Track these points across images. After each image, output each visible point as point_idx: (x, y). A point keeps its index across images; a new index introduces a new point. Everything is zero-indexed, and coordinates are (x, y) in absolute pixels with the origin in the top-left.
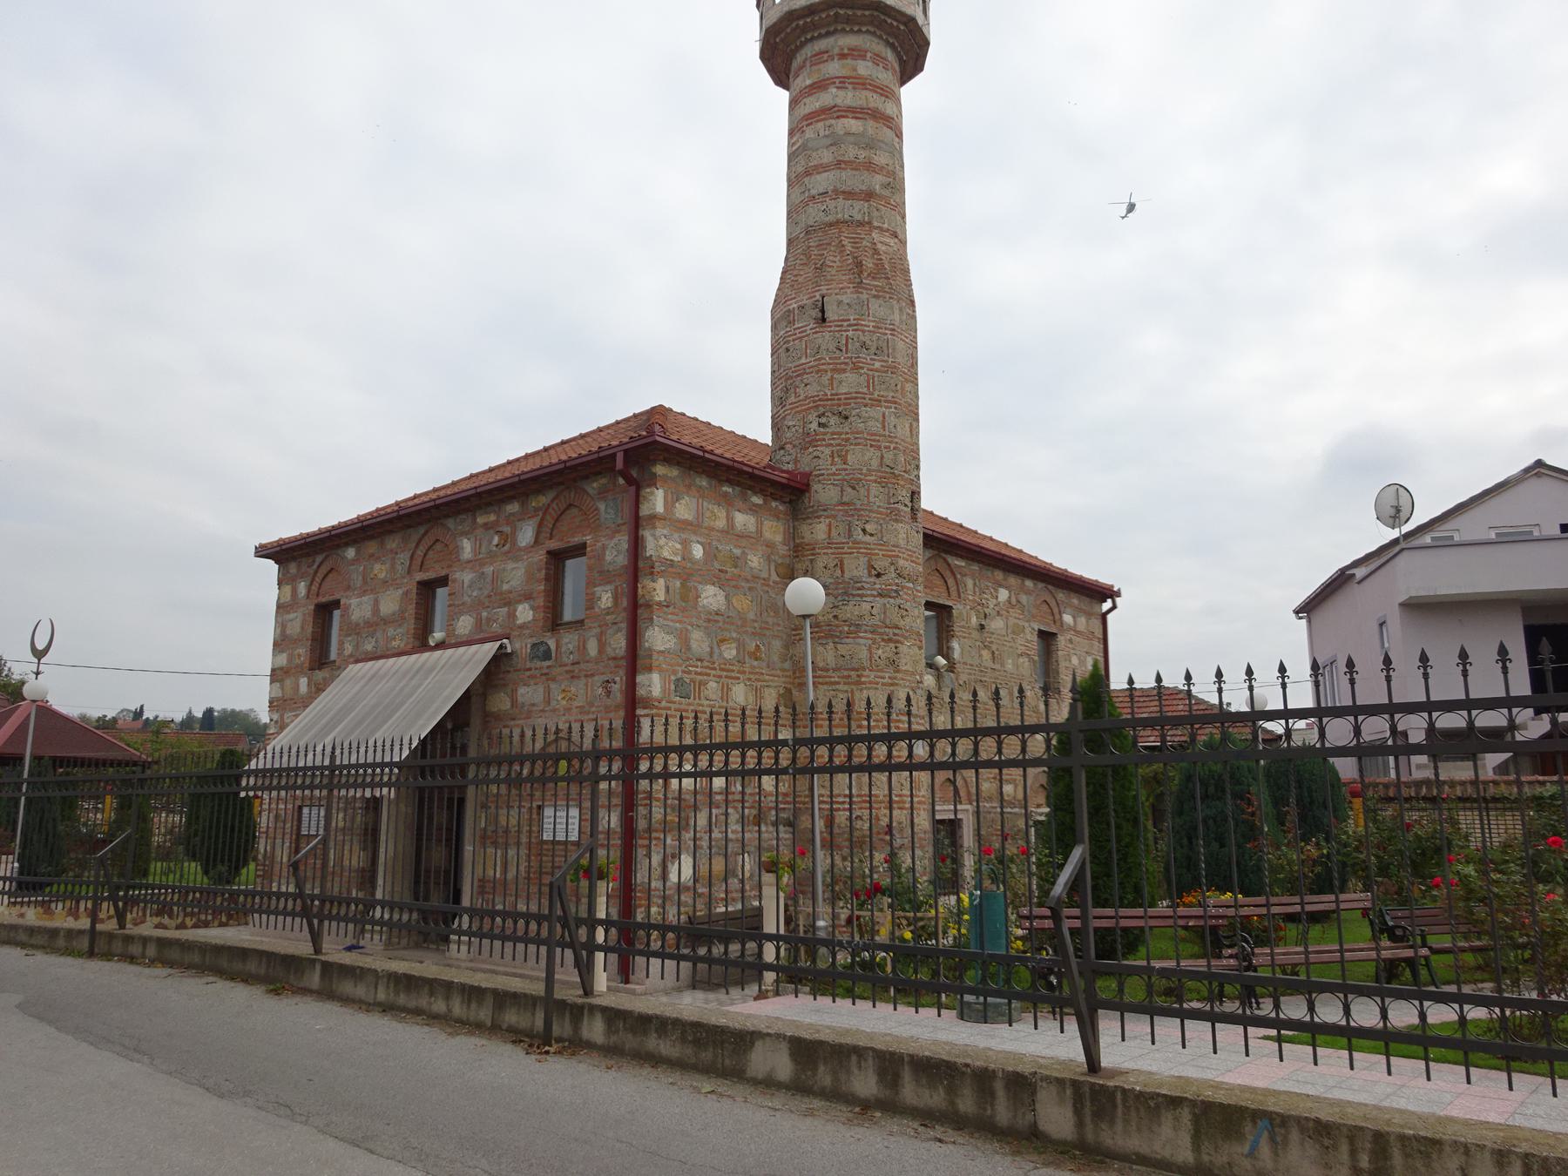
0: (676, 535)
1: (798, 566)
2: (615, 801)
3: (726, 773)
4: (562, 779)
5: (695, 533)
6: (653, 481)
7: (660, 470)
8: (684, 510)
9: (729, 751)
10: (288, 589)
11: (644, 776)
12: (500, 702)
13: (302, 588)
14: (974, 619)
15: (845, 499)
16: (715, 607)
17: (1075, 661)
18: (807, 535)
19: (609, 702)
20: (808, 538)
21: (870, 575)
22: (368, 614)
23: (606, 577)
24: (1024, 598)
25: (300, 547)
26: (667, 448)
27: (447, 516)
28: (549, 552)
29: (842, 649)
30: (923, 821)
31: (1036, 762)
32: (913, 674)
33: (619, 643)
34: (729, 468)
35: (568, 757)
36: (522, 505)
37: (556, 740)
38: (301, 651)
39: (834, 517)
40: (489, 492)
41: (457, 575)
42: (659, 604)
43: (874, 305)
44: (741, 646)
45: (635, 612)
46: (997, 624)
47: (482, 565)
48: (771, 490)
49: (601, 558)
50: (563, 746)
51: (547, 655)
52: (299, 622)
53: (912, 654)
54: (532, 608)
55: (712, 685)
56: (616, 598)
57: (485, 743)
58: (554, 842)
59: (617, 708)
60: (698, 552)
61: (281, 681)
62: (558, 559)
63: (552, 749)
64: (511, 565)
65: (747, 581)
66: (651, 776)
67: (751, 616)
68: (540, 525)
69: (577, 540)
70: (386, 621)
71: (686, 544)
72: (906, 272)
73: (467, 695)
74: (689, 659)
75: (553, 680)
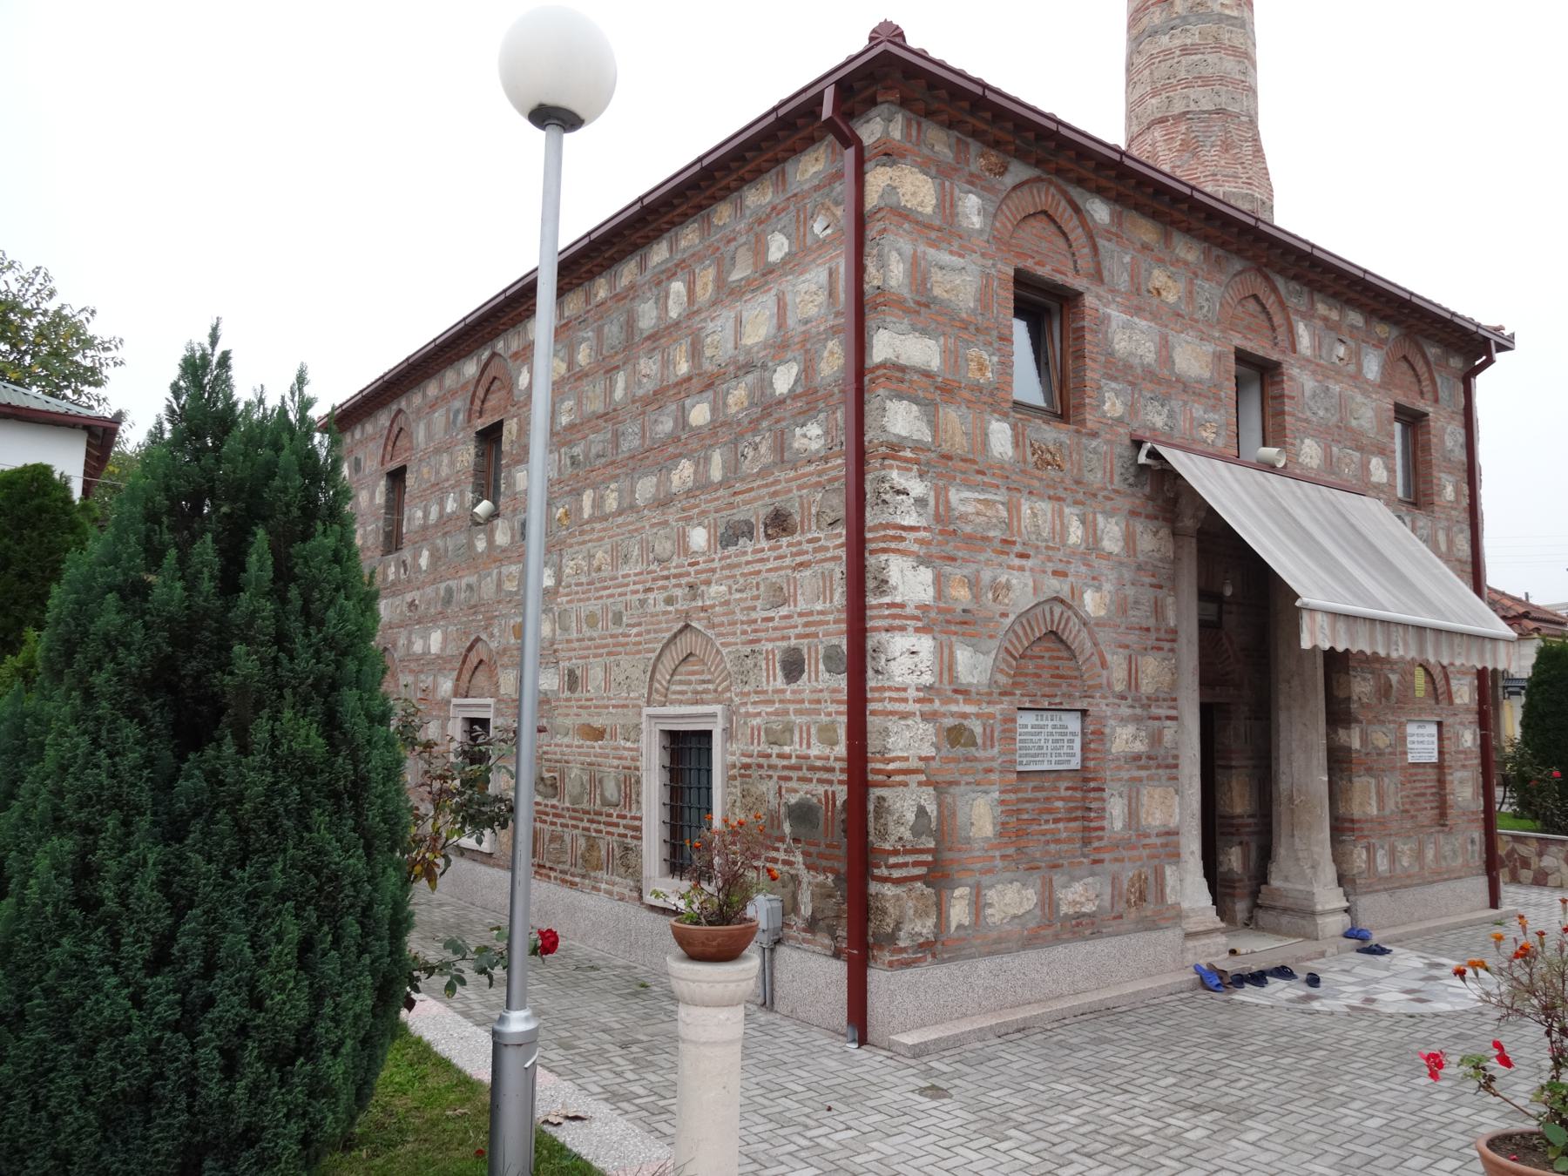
27: (1282, 272)
41: (1295, 372)
56: (1457, 491)
64: (1359, 398)
69: (1421, 405)
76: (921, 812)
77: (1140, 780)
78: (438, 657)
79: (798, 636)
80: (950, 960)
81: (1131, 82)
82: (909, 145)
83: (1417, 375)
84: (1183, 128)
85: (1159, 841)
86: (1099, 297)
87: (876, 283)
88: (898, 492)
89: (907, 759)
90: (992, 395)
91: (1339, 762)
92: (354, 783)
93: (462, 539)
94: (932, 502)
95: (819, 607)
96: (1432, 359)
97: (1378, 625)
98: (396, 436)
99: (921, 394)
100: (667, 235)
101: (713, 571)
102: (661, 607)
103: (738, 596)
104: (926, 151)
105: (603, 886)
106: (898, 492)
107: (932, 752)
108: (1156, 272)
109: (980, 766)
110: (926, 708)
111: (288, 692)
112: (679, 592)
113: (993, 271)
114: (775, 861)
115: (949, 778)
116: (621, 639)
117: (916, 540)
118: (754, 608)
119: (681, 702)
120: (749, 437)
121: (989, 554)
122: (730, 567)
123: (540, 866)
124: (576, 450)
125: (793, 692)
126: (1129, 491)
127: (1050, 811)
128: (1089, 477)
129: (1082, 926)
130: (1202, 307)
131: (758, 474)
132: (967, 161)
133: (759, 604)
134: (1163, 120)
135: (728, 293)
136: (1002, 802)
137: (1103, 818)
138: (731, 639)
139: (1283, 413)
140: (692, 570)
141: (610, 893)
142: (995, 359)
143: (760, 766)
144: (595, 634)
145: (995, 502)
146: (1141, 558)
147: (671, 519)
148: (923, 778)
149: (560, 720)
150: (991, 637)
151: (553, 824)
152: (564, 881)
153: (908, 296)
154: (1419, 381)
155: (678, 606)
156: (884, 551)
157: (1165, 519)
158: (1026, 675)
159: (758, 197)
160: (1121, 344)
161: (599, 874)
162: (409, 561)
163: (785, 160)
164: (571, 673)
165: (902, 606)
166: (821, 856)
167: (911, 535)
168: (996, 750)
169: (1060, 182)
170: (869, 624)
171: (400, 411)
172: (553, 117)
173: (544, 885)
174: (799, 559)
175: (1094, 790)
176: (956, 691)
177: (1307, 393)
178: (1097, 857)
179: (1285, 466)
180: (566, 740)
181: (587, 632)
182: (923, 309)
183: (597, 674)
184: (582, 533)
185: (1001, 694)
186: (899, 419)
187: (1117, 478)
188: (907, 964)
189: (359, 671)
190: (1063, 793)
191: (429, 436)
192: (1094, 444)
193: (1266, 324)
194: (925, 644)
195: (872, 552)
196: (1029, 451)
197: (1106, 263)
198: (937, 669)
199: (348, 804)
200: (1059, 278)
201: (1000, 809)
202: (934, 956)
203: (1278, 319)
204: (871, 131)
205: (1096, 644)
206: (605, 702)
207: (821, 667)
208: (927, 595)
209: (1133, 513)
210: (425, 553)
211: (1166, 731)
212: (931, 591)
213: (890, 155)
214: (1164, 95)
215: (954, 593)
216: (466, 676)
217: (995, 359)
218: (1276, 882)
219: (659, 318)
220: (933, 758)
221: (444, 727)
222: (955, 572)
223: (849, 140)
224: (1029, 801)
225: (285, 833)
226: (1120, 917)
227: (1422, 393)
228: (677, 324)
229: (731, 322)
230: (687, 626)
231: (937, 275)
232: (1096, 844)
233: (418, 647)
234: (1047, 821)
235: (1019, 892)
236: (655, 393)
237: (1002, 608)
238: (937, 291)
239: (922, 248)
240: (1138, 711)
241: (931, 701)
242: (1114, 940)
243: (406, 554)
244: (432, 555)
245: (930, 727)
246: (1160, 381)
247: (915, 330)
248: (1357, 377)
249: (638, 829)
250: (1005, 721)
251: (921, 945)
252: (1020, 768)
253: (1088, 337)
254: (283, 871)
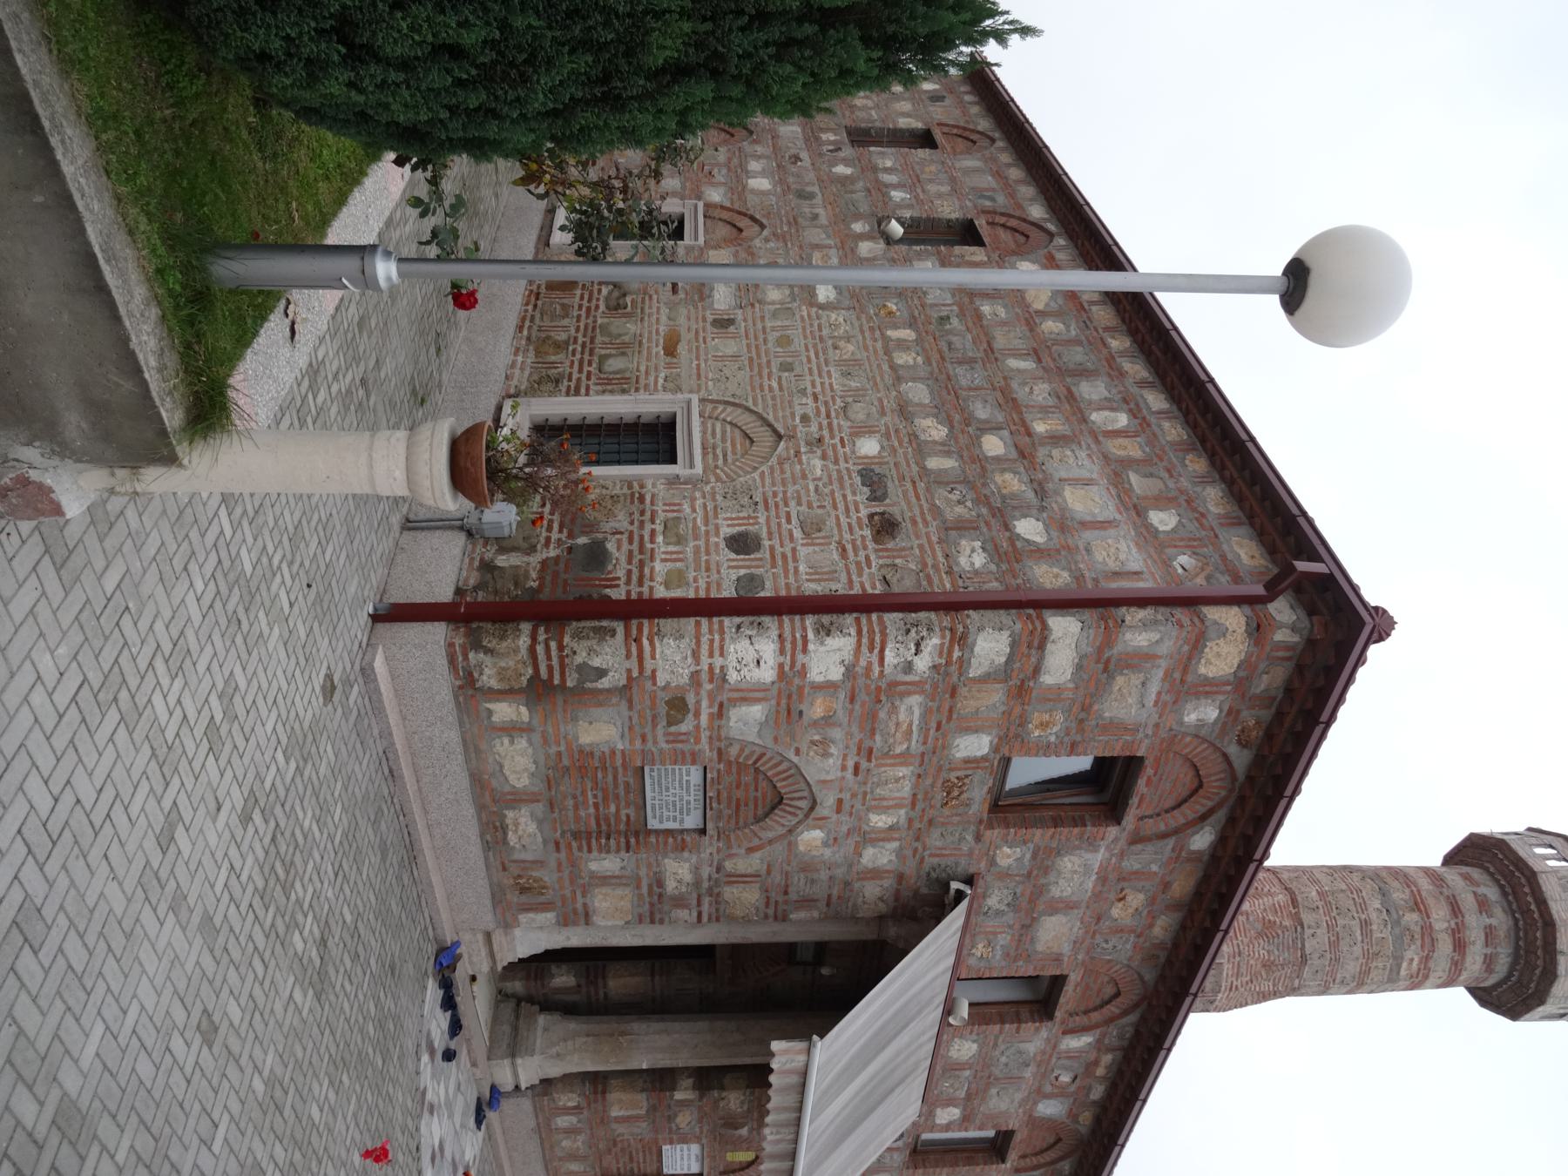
27: (1143, 1019)
36: (1094, 1102)
41: (1044, 1033)
64: (1019, 1096)
69: (1013, 1156)
76: (602, 673)
77: (638, 887)
78: (744, 187)
79: (772, 548)
80: (458, 703)
81: (1333, 871)
82: (1268, 648)
83: (1042, 1152)
84: (1287, 923)
85: (579, 906)
86: (1116, 840)
87: (1128, 618)
88: (918, 645)
89: (653, 657)
90: (1017, 736)
91: (660, 1080)
92: (619, 97)
93: (864, 208)
94: (908, 678)
95: (801, 568)
96: (1058, 1166)
97: (795, 1115)
98: (967, 137)
99: (1018, 665)
100: (1175, 408)
101: (836, 462)
102: (799, 411)
103: (812, 488)
104: (1262, 666)
105: (520, 359)
106: (918, 645)
107: (661, 682)
108: (1141, 896)
109: (648, 730)
110: (704, 676)
111: (708, 26)
112: (814, 428)
113: (1141, 735)
114: (550, 529)
115: (636, 699)
116: (766, 371)
117: (870, 663)
118: (799, 504)
119: (704, 432)
120: (971, 495)
121: (858, 736)
122: (841, 479)
123: (538, 294)
124: (955, 322)
125: (717, 544)
126: (923, 873)
127: (606, 799)
128: (935, 833)
129: (494, 833)
130: (1106, 942)
131: (934, 505)
132: (1252, 708)
133: (804, 508)
134: (1294, 902)
135: (1117, 471)
136: (613, 752)
137: (600, 851)
138: (768, 481)
139: (1003, 1022)
140: (837, 440)
141: (513, 365)
142: (1053, 739)
143: (642, 513)
144: (770, 345)
145: (909, 740)
146: (857, 885)
147: (888, 419)
148: (635, 674)
149: (683, 311)
150: (776, 739)
151: (580, 307)
152: (523, 319)
153: (1115, 651)
154: (1036, 1154)
155: (800, 428)
156: (859, 632)
157: (895, 908)
158: (739, 773)
159: (1213, 499)
160: (1069, 863)
161: (531, 354)
162: (842, 154)
163: (1252, 525)
164: (731, 322)
165: (805, 650)
166: (556, 575)
167: (875, 658)
168: (664, 746)
169: (1231, 801)
170: (786, 619)
171: (993, 140)
172: (1296, 284)
173: (519, 299)
174: (849, 547)
175: (628, 843)
176: (721, 705)
178: (562, 846)
179: (950, 1025)
180: (664, 319)
181: (773, 336)
182: (1102, 666)
183: (730, 347)
184: (872, 329)
185: (719, 750)
186: (991, 645)
187: (935, 860)
188: (452, 661)
189: (731, 99)
190: (623, 812)
191: (968, 172)
192: (969, 838)
193: (1091, 1006)
194: (767, 674)
195: (858, 620)
196: (961, 774)
197: (1150, 847)
198: (743, 686)
199: (598, 91)
200: (1134, 801)
201: (606, 750)
202: (461, 687)
203: (1096, 1017)
204: (1282, 611)
205: (770, 842)
206: (702, 357)
207: (742, 572)
208: (816, 674)
209: (900, 877)
210: (849, 171)
211: (686, 911)
212: (819, 679)
213: (1258, 630)
214: (1320, 904)
215: (819, 701)
216: (725, 215)
217: (1053, 739)
218: (542, 1020)
219: (1090, 402)
220: (655, 684)
221: (674, 194)
222: (840, 702)
223: (1273, 589)
224: (615, 778)
225: (567, 27)
226: (504, 869)
227: (1023, 1157)
228: (1084, 420)
229: (1085, 474)
230: (780, 437)
231: (1136, 679)
232: (574, 844)
233: (754, 166)
234: (595, 796)
235: (526, 770)
236: (1014, 400)
237: (804, 749)
238: (1120, 680)
239: (1163, 663)
240: (706, 885)
241: (711, 681)
242: (481, 863)
243: (848, 151)
244: (847, 177)
245: (686, 679)
246: (1032, 902)
247: (1081, 658)
248: (1040, 1094)
249: (577, 393)
250: (693, 754)
251: (470, 674)
252: (647, 769)
253: (1076, 830)
254: (530, 26)
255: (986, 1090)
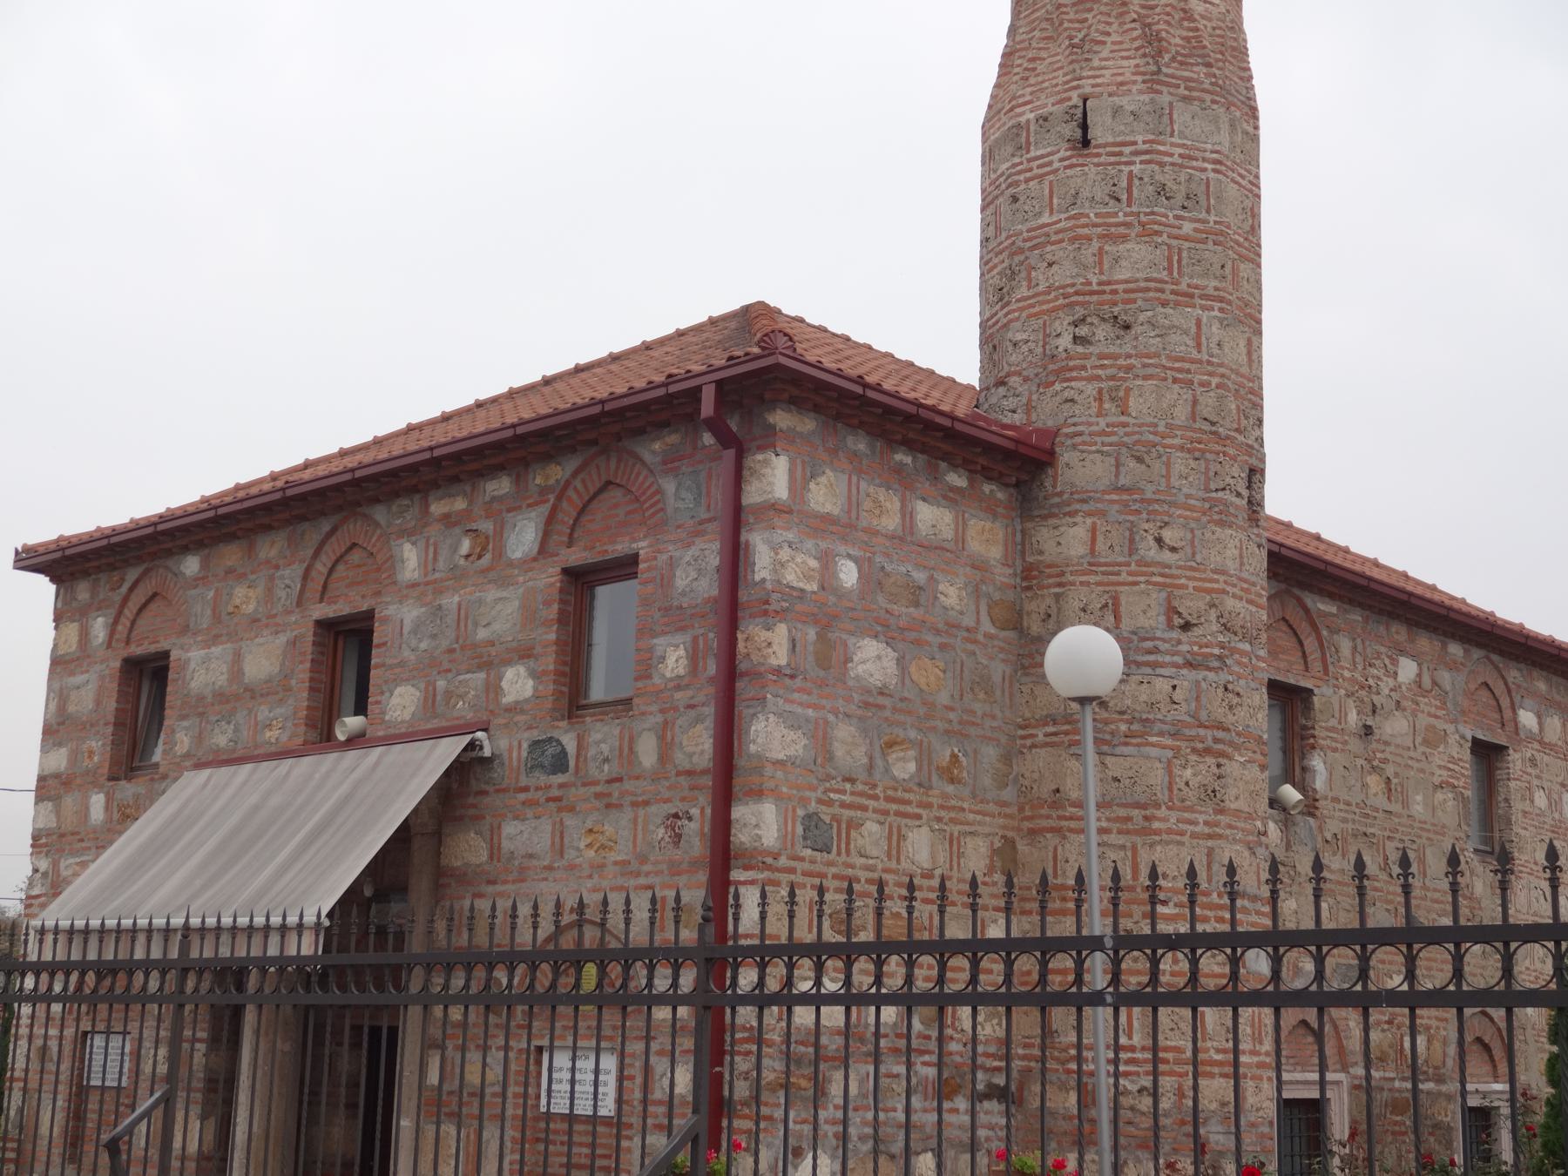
0: (809, 544)
1: (1031, 606)
2: (687, 1043)
3: (907, 1000)
4: (588, 999)
5: (844, 539)
6: (770, 440)
7: (781, 419)
8: (825, 495)
9: (901, 956)
10: (72, 630)
11: (745, 1000)
12: (468, 849)
13: (99, 628)
14: (1353, 717)
15: (1123, 481)
16: (876, 680)
17: (1541, 800)
18: (1049, 547)
19: (677, 854)
20: (1051, 551)
21: (1170, 626)
22: (222, 680)
23: (676, 618)
24: (1445, 677)
25: (97, 553)
26: (797, 379)
28: (566, 571)
29: (1116, 766)
30: (1261, 1102)
31: (1533, 998)
32: (1250, 817)
33: (699, 744)
34: (909, 418)
35: (602, 958)
36: (517, 481)
37: (579, 924)
38: (95, 744)
39: (1102, 514)
40: (457, 457)
41: (391, 610)
42: (778, 671)
43: (1182, 115)
44: (924, 756)
45: (731, 688)
46: (1395, 727)
47: (439, 589)
48: (982, 461)
49: (666, 582)
50: (591, 936)
51: (560, 763)
52: (95, 690)
53: (1247, 778)
54: (533, 674)
55: (871, 827)
56: (694, 658)
57: (441, 926)
58: (571, 1118)
59: (694, 865)
60: (848, 574)
61: (56, 799)
62: (581, 582)
63: (567, 942)
64: (492, 594)
65: (938, 632)
66: (761, 1000)
67: (943, 698)
68: (550, 520)
69: (621, 548)
70: (253, 693)
71: (827, 560)
72: (1241, 52)
73: (403, 835)
74: (829, 778)
75: (571, 809)
177: (406, 630)
200: (153, 648)
255: (474, 646)
